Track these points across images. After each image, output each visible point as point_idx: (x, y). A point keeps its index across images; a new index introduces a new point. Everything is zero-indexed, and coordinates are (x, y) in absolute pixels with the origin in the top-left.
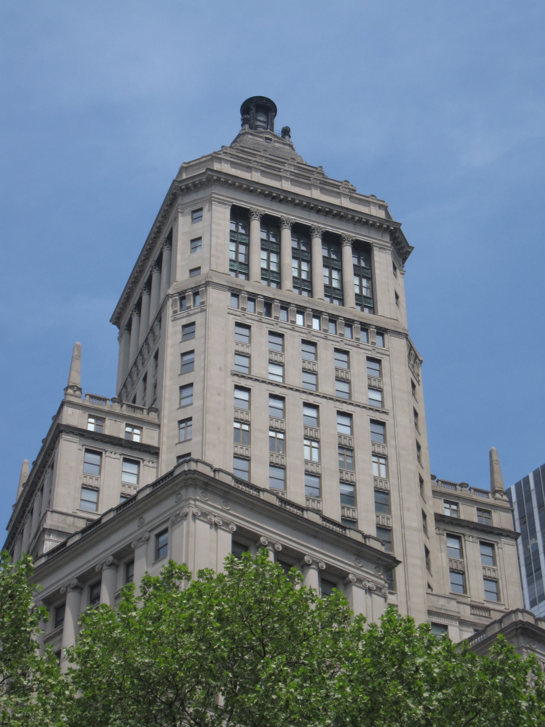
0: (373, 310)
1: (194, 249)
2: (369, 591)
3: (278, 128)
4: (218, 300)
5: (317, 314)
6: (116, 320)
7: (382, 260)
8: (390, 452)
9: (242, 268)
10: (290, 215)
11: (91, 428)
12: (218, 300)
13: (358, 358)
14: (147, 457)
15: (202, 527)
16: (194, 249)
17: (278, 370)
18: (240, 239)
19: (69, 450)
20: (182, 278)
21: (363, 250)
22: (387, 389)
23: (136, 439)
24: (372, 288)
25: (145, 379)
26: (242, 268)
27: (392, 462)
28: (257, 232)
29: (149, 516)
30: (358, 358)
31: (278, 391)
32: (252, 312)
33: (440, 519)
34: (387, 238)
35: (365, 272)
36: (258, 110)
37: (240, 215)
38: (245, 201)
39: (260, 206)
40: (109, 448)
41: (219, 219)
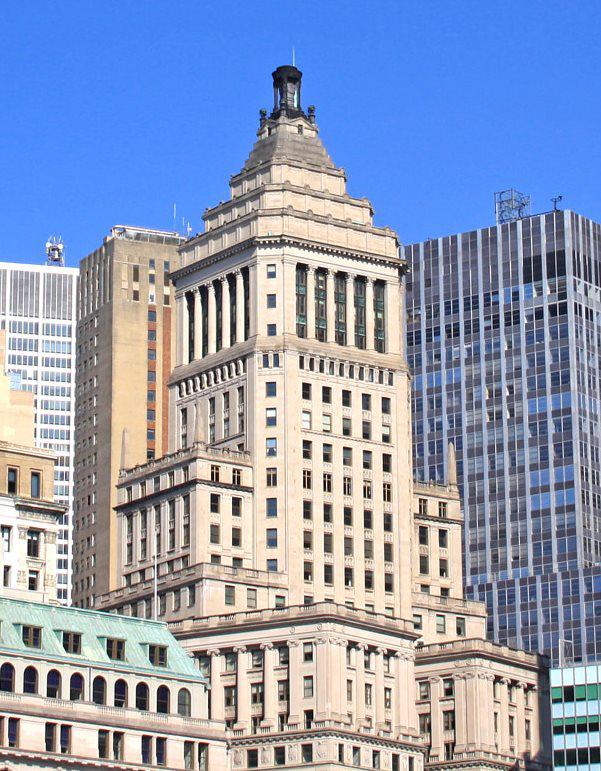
12: (290, 360)
15: (334, 647)
37: (302, 268)
39: (315, 260)
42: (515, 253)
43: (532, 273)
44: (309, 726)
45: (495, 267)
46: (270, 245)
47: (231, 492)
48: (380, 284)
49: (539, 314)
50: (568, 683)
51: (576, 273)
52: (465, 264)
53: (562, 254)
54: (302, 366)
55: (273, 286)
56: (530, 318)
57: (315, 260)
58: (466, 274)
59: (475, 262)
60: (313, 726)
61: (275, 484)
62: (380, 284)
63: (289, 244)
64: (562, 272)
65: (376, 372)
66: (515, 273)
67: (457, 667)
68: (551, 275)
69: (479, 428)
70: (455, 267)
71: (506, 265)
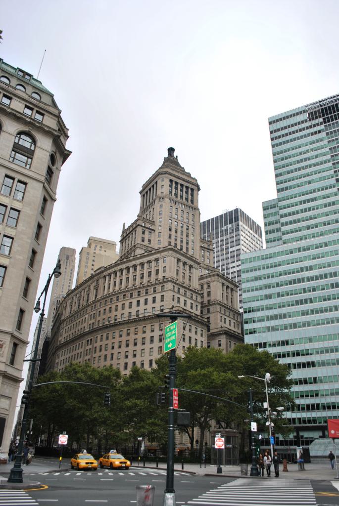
0: (193, 204)
1: (162, 188)
2: (196, 269)
3: (175, 156)
4: (167, 200)
5: (184, 205)
6: (141, 193)
7: (195, 192)
8: (195, 234)
9: (171, 192)
10: (180, 182)
11: (143, 225)
13: (190, 215)
16: (162, 188)
17: (177, 216)
18: (171, 186)
19: (139, 230)
20: (159, 193)
21: (192, 190)
22: (195, 221)
23: (151, 228)
24: (193, 198)
26: (171, 192)
27: (195, 236)
28: (174, 185)
29: (163, 254)
30: (190, 215)
31: (176, 221)
32: (173, 205)
33: (201, 247)
35: (192, 195)
36: (171, 150)
37: (171, 181)
38: (172, 178)
46: (163, 174)
60: (165, 280)
62: (192, 190)
64: (238, 220)
68: (235, 221)
69: (219, 256)
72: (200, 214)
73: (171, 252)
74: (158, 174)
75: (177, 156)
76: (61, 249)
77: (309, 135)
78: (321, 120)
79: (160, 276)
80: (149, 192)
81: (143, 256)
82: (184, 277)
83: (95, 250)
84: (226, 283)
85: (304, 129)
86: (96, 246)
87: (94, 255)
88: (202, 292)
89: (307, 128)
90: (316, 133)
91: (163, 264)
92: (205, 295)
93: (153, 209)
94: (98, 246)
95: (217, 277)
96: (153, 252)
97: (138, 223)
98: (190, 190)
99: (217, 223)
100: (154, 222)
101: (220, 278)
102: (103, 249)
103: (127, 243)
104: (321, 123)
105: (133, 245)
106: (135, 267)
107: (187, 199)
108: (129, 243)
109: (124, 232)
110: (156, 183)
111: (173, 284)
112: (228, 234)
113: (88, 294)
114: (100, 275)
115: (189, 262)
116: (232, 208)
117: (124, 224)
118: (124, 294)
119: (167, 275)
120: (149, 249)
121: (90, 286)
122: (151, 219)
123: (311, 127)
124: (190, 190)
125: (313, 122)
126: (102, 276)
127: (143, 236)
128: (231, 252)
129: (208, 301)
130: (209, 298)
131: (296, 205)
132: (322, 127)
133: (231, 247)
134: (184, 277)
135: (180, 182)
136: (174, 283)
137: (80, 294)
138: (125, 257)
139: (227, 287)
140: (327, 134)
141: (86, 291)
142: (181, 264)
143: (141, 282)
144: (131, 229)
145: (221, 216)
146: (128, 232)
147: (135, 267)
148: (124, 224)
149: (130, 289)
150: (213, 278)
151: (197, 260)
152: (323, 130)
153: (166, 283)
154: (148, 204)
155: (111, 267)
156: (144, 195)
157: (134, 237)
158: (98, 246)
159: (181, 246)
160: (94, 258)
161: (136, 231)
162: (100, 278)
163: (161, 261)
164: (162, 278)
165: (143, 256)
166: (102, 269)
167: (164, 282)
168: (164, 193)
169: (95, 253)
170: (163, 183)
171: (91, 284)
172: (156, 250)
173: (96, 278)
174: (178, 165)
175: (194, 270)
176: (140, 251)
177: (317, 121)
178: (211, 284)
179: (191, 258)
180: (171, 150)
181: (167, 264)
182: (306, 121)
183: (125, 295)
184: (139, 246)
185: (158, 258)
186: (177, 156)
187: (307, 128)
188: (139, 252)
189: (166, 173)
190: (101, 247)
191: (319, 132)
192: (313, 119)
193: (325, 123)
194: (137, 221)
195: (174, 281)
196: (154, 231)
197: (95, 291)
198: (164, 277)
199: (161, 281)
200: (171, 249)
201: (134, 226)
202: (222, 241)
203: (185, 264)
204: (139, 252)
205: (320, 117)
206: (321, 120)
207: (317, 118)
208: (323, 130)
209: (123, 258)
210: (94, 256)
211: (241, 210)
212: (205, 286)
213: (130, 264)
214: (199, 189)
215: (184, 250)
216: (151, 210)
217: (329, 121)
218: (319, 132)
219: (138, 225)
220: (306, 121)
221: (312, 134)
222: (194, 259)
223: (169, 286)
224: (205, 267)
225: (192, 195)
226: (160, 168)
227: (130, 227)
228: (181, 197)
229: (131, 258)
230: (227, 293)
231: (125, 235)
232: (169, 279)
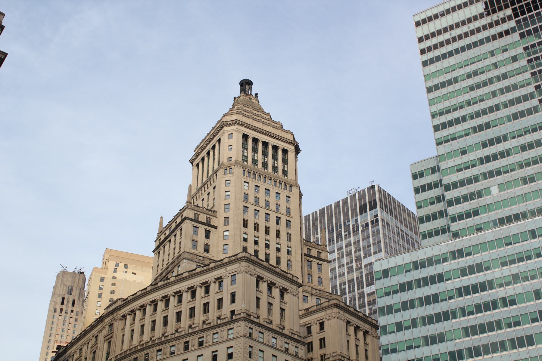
0: (287, 176)
4: (238, 171)
7: (291, 155)
9: (245, 159)
14: (213, 229)
18: (245, 147)
19: (188, 226)
21: (285, 151)
25: (209, 194)
26: (245, 159)
34: (293, 148)
35: (285, 161)
36: (246, 84)
37: (245, 137)
40: (201, 225)
41: (237, 139)
42: (356, 205)
43: (363, 210)
44: (232, 318)
45: (348, 212)
46: (230, 125)
47: (205, 227)
48: (285, 151)
49: (367, 225)
50: (385, 267)
51: (381, 207)
52: (336, 214)
53: (375, 201)
54: (244, 174)
55: (231, 142)
56: (362, 226)
57: (252, 134)
58: (336, 217)
59: (340, 212)
60: (234, 317)
61: (228, 225)
63: (238, 124)
65: (283, 184)
66: (356, 212)
67: (326, 314)
68: (371, 209)
69: (344, 274)
70: (332, 216)
71: (352, 210)
72: (301, 195)
73: (244, 264)
74: (221, 126)
75: (256, 95)
76: (59, 275)
77: (488, 40)
78: (509, 12)
79: (226, 311)
80: (206, 159)
81: (192, 274)
82: (270, 311)
83: (115, 271)
84: (355, 321)
85: (478, 30)
86: (117, 265)
87: (114, 281)
88: (309, 340)
89: (485, 28)
90: (501, 35)
91: (230, 287)
92: (316, 345)
93: (214, 188)
94: (122, 265)
95: (336, 310)
96: (212, 265)
97: (185, 214)
98: (280, 152)
99: (338, 213)
100: (214, 211)
101: (342, 312)
102: (130, 270)
103: (167, 252)
104: (510, 18)
105: (177, 255)
106: (179, 295)
107: (275, 169)
108: (169, 252)
109: (160, 233)
110: (219, 141)
111: (250, 325)
112: (358, 233)
113: (94, 353)
114: (115, 315)
115: (280, 282)
116: (364, 186)
117: (162, 217)
118: (158, 348)
119: (238, 307)
120: (207, 262)
121: (96, 337)
122: (209, 208)
123: (491, 25)
124: (280, 152)
125: (495, 17)
126: (119, 317)
127: (195, 238)
128: (366, 266)
129: (321, 356)
130: (323, 351)
131: (474, 166)
132: (512, 24)
133: (365, 257)
134: (270, 311)
135: (262, 138)
136: (253, 322)
137: (81, 353)
138: (163, 279)
139: (357, 328)
140: (522, 36)
141: (90, 345)
142: (264, 286)
143: (190, 323)
144: (173, 226)
145: (345, 201)
146: (168, 232)
147: (179, 295)
148: (162, 217)
149: (169, 338)
150: (329, 311)
151: (294, 279)
152: (513, 30)
153: (236, 323)
154: (205, 180)
155: (135, 297)
156: (198, 165)
157: (178, 241)
158: (122, 265)
159: (267, 255)
160: (113, 288)
161: (181, 230)
162: (116, 320)
163: (227, 282)
164: (229, 315)
165: (192, 274)
166: (119, 303)
167: (232, 321)
168: (233, 159)
169: (115, 278)
170: (231, 142)
171: (100, 331)
172: (216, 262)
173: (107, 320)
174: (260, 109)
175: (287, 297)
176: (188, 265)
177: (501, 15)
178: (326, 324)
179: (282, 275)
180: (246, 84)
181: (238, 288)
182: (482, 16)
183: (159, 350)
184: (186, 256)
185: (221, 278)
186: (256, 95)
187: (485, 28)
188: (186, 266)
189: (237, 123)
190: (126, 266)
191: (507, 33)
192: (494, 11)
193: (516, 16)
194: (184, 209)
195: (252, 318)
196: (216, 227)
197: (106, 345)
198: (233, 312)
199: (226, 320)
200: (248, 260)
201: (179, 220)
202: (348, 245)
203: (271, 285)
204: (186, 266)
205: (507, 7)
206: (509, 12)
207: (500, 9)
208: (513, 30)
209: (158, 280)
210: (113, 284)
211: (379, 188)
212: (315, 328)
213: (170, 291)
214: (297, 151)
215: (273, 261)
216: (211, 190)
217: (523, 13)
218: (507, 33)
219: (186, 218)
220: (482, 16)
221: (494, 38)
222: (291, 277)
223: (241, 328)
224: (314, 292)
225: (285, 161)
226: (225, 115)
227: (170, 223)
228: (265, 165)
229: (172, 279)
230: (357, 339)
231: (162, 238)
232: (242, 315)
